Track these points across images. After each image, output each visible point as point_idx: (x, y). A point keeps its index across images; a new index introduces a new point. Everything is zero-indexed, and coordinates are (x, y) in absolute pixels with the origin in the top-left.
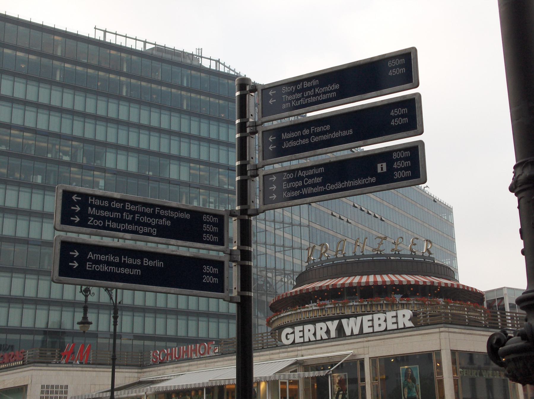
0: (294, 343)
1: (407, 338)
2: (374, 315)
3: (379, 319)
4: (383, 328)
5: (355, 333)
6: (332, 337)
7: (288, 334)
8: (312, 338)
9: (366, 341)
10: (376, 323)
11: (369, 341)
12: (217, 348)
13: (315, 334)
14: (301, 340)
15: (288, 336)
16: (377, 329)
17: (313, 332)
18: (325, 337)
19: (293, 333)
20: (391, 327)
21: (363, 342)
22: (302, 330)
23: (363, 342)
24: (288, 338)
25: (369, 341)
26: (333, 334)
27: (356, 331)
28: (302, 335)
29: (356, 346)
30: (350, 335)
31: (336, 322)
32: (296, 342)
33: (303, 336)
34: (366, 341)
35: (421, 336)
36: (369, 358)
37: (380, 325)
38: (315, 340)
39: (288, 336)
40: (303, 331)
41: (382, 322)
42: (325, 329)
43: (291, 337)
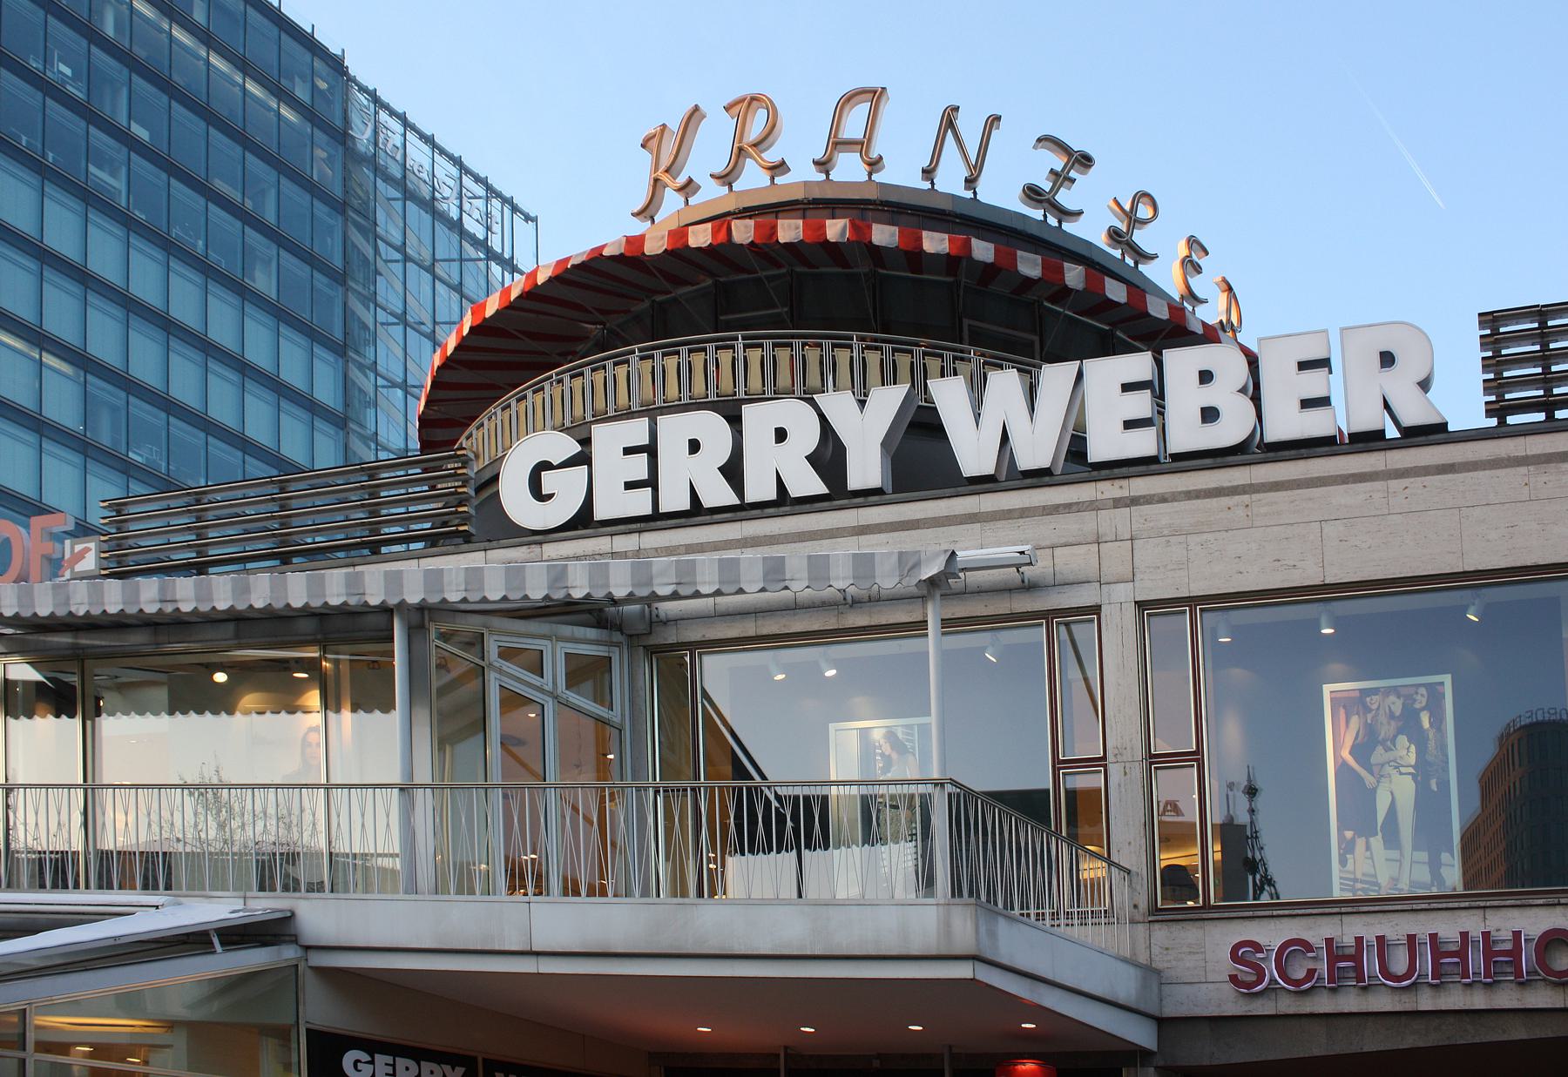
0: (583, 521)
1: (1415, 483)
2: (1171, 356)
3: (1206, 377)
4: (1229, 431)
5: (1025, 462)
6: (855, 481)
7: (545, 466)
8: (718, 493)
9: (1118, 503)
10: (1184, 398)
11: (1134, 501)
12: (87, 550)
13: (733, 471)
14: (640, 503)
15: (546, 476)
16: (1186, 434)
17: (724, 456)
18: (807, 483)
19: (583, 459)
20: (1285, 423)
21: (1094, 506)
22: (645, 441)
23: (1094, 506)
24: (545, 491)
25: (1134, 501)
26: (865, 469)
27: (1034, 448)
28: (643, 474)
29: (1046, 529)
30: (988, 468)
31: (888, 401)
32: (600, 513)
33: (652, 482)
34: (1118, 503)
35: (1523, 470)
36: (1142, 606)
37: (1209, 415)
38: (733, 500)
39: (546, 476)
40: (651, 450)
41: (1226, 394)
42: (806, 437)
43: (567, 490)
